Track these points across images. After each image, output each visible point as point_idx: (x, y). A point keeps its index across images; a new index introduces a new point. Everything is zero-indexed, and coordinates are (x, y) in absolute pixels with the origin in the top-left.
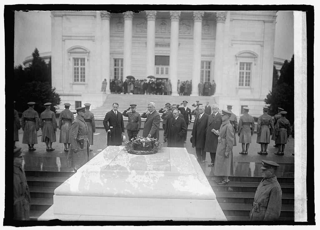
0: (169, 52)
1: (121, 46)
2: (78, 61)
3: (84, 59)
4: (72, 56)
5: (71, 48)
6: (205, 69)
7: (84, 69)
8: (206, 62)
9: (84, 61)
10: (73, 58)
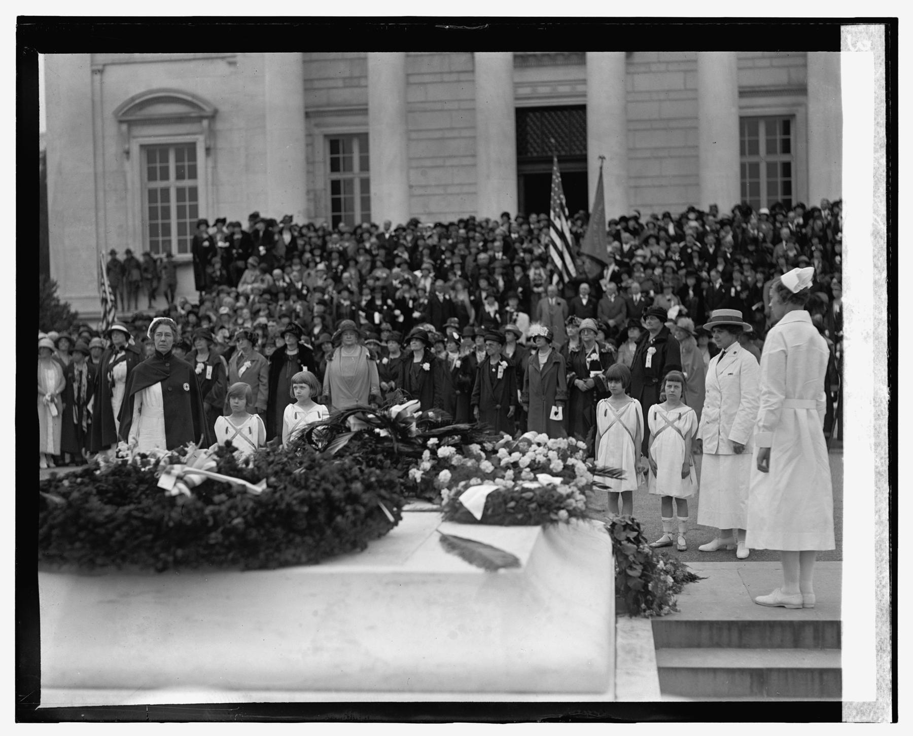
0: (580, 88)
1: (359, 78)
2: (165, 159)
3: (192, 147)
4: (135, 137)
5: (133, 99)
6: (763, 157)
7: (194, 191)
8: (769, 120)
9: (193, 157)
10: (142, 146)
